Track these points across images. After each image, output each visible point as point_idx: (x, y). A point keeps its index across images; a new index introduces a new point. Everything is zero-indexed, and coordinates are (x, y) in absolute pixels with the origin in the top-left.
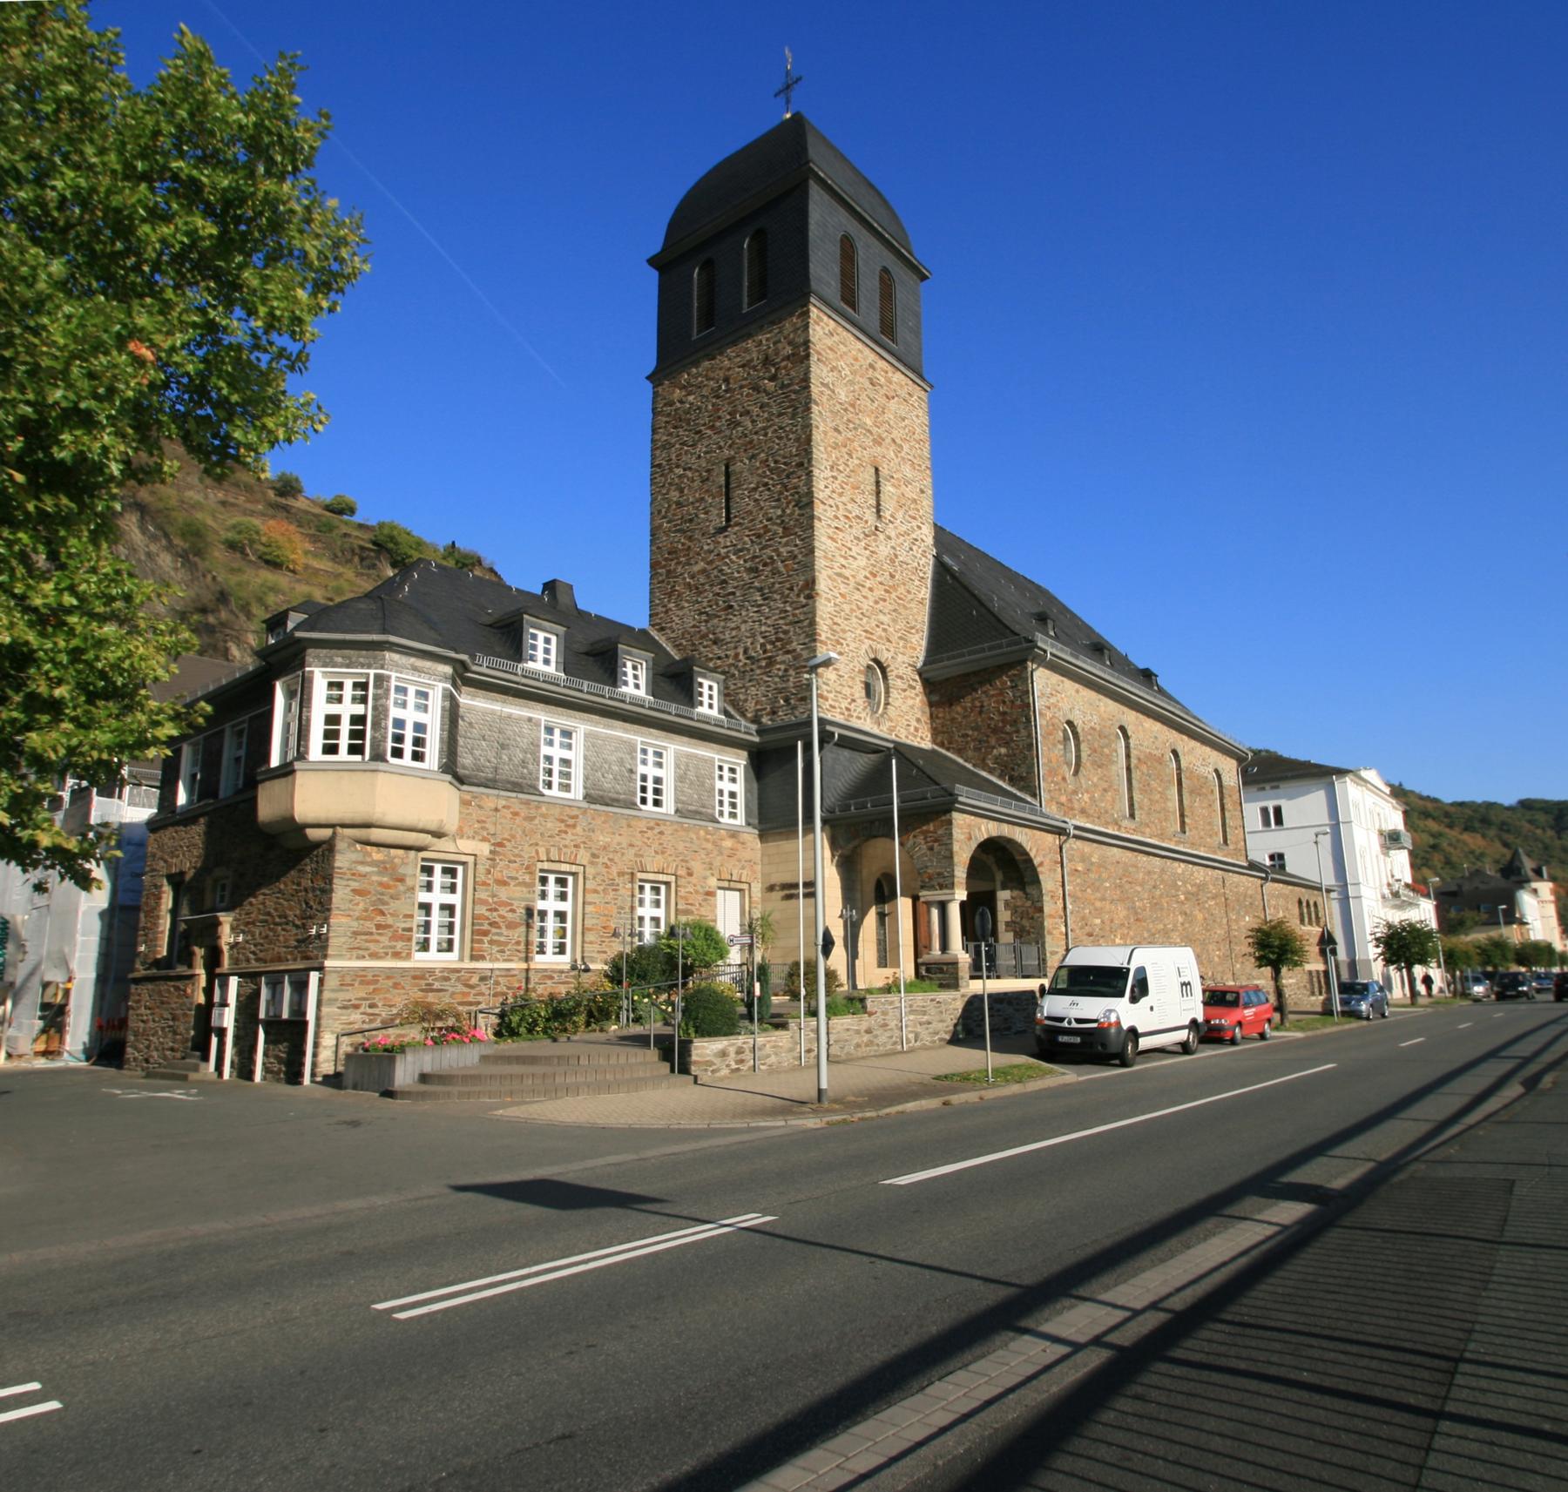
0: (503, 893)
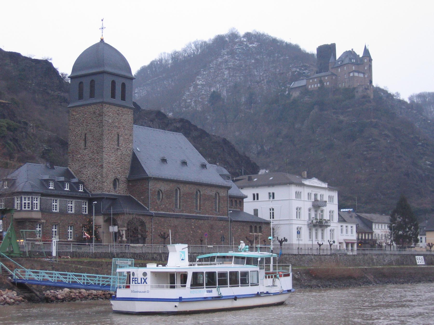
0: (47, 228)
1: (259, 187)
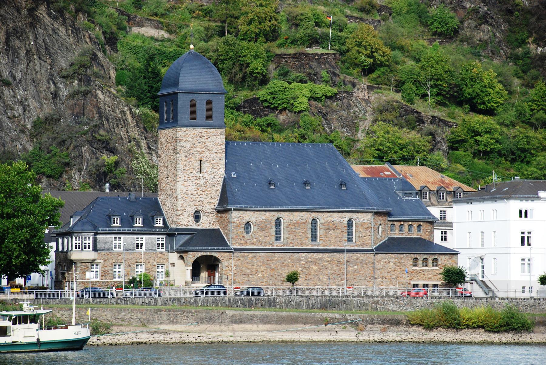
0: (106, 269)
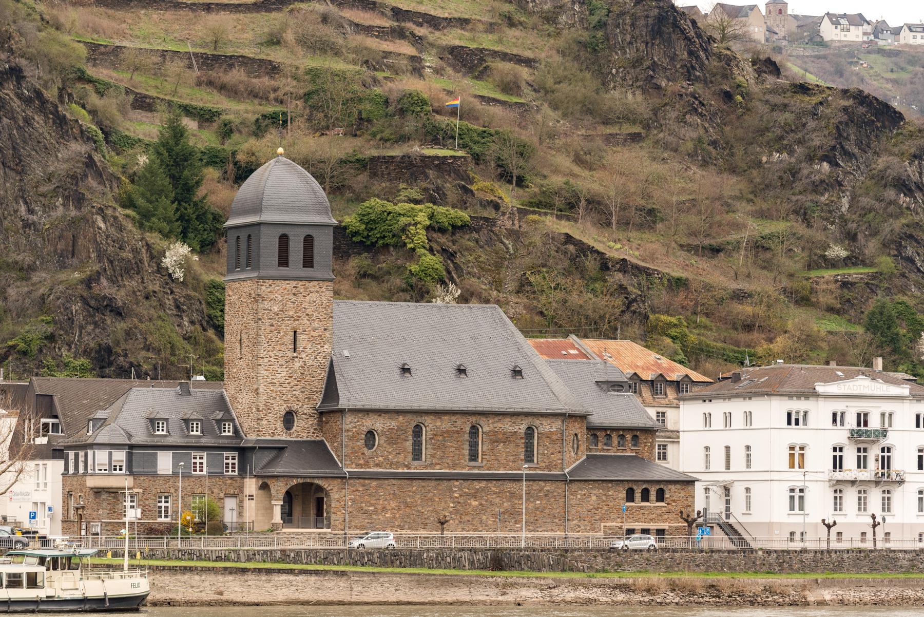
0: (147, 502)
1: (732, 400)
